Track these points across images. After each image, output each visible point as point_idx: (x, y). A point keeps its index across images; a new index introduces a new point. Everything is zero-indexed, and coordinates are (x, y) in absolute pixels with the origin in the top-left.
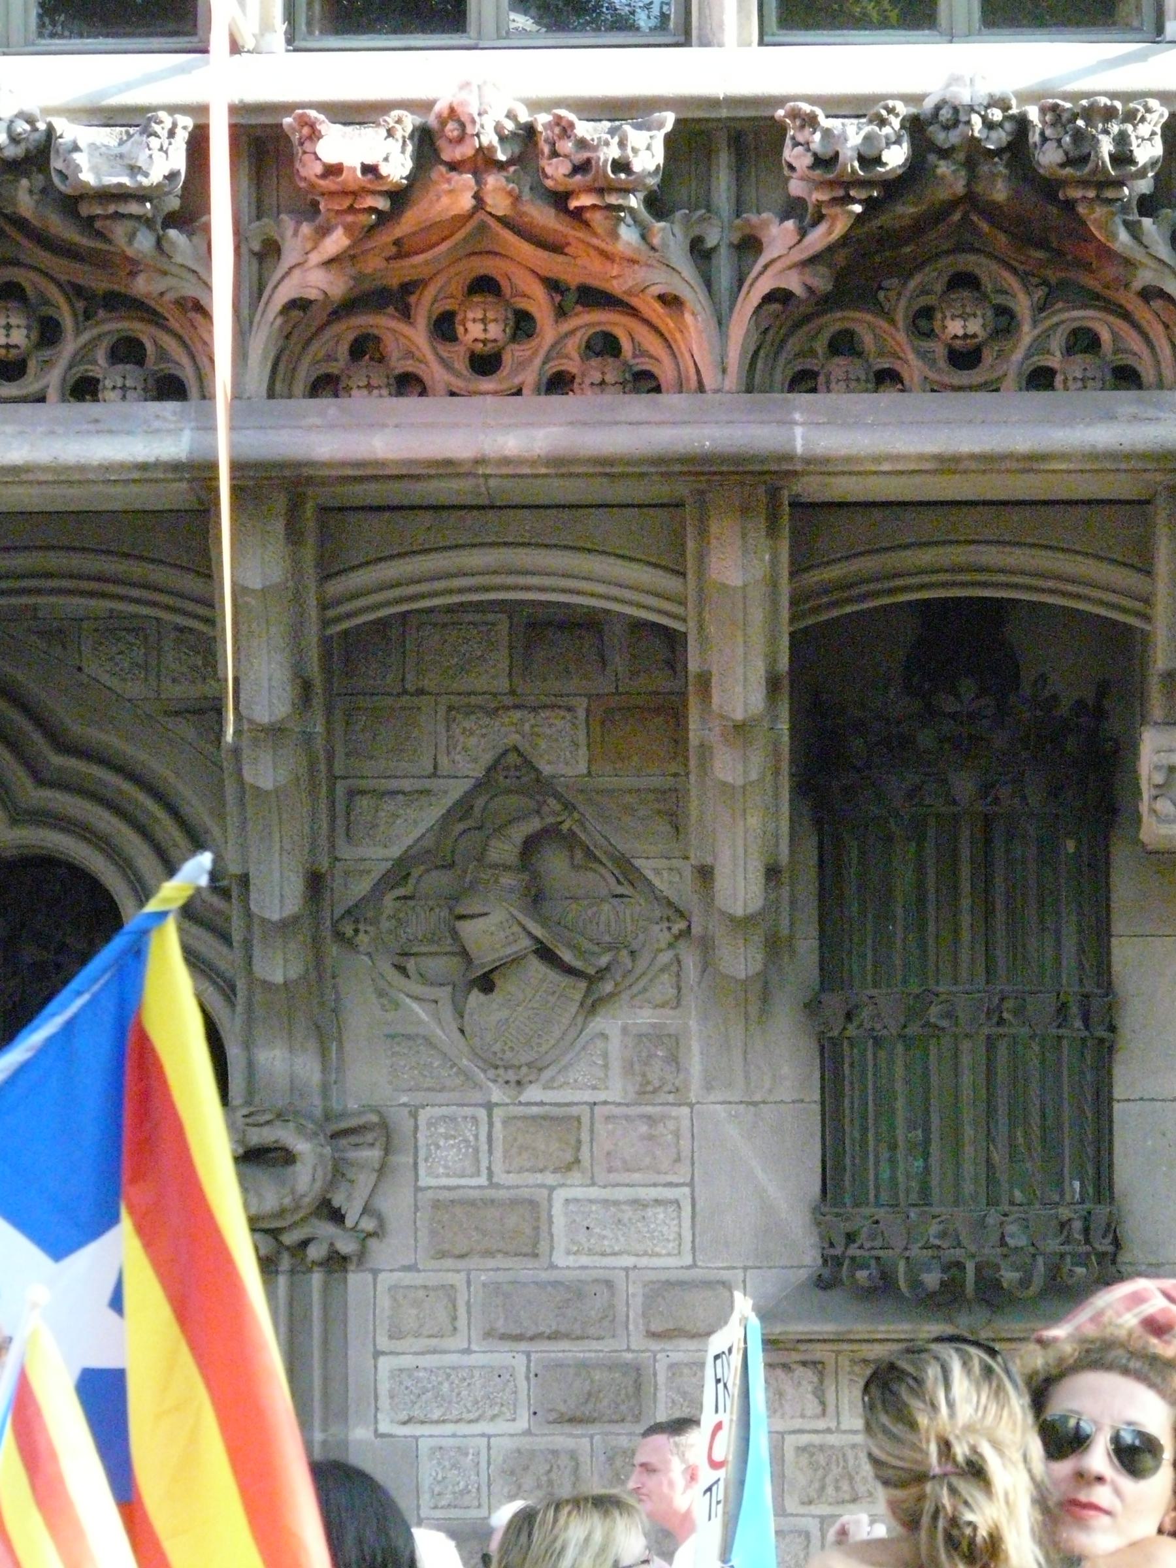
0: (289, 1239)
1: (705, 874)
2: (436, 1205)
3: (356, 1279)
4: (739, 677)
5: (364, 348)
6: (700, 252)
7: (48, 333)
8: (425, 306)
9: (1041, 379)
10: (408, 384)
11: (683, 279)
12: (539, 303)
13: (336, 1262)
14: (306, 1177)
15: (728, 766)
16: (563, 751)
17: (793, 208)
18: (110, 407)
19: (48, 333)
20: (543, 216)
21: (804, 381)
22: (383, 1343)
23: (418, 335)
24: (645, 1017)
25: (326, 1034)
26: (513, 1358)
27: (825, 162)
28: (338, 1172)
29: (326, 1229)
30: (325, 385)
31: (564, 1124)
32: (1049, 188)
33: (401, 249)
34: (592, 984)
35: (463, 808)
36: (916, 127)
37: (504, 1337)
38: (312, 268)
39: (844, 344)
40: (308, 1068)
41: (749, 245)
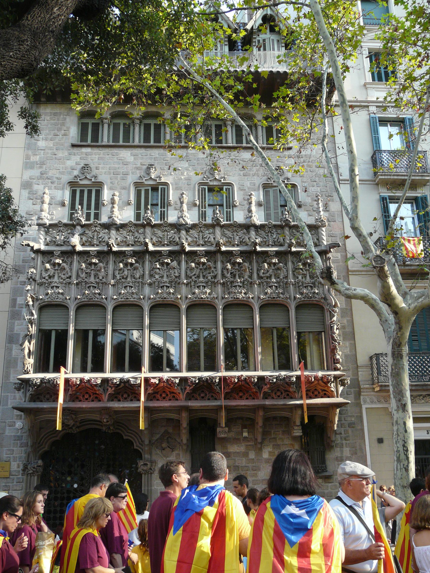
1: (182, 440)
3: (153, 475)
4: (185, 424)
5: (154, 397)
6: (181, 389)
7: (129, 396)
8: (160, 393)
9: (209, 399)
10: (158, 400)
11: (180, 391)
12: (169, 393)
13: (151, 473)
14: (149, 466)
15: (184, 431)
16: (170, 430)
17: (189, 386)
18: (134, 402)
19: (129, 396)
20: (169, 386)
21: (190, 399)
23: (159, 396)
24: (177, 452)
25: (151, 454)
27: (192, 382)
28: (152, 466)
30: (151, 400)
32: (209, 384)
33: (157, 389)
34: (173, 450)
35: (162, 435)
36: (199, 379)
38: (150, 391)
39: (193, 396)
40: (149, 457)
41: (186, 389)
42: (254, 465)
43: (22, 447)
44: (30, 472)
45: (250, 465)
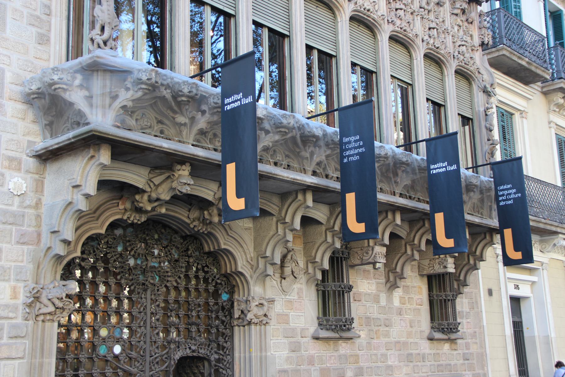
0: (260, 320)
2: (277, 315)
3: (267, 327)
22: (272, 338)
26: (285, 341)
29: (265, 318)
31: (290, 302)
37: (286, 337)
42: (385, 316)
43: (23, 243)
44: (44, 310)
45: (382, 316)
